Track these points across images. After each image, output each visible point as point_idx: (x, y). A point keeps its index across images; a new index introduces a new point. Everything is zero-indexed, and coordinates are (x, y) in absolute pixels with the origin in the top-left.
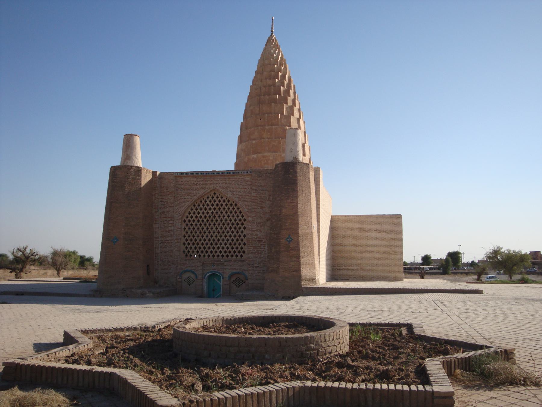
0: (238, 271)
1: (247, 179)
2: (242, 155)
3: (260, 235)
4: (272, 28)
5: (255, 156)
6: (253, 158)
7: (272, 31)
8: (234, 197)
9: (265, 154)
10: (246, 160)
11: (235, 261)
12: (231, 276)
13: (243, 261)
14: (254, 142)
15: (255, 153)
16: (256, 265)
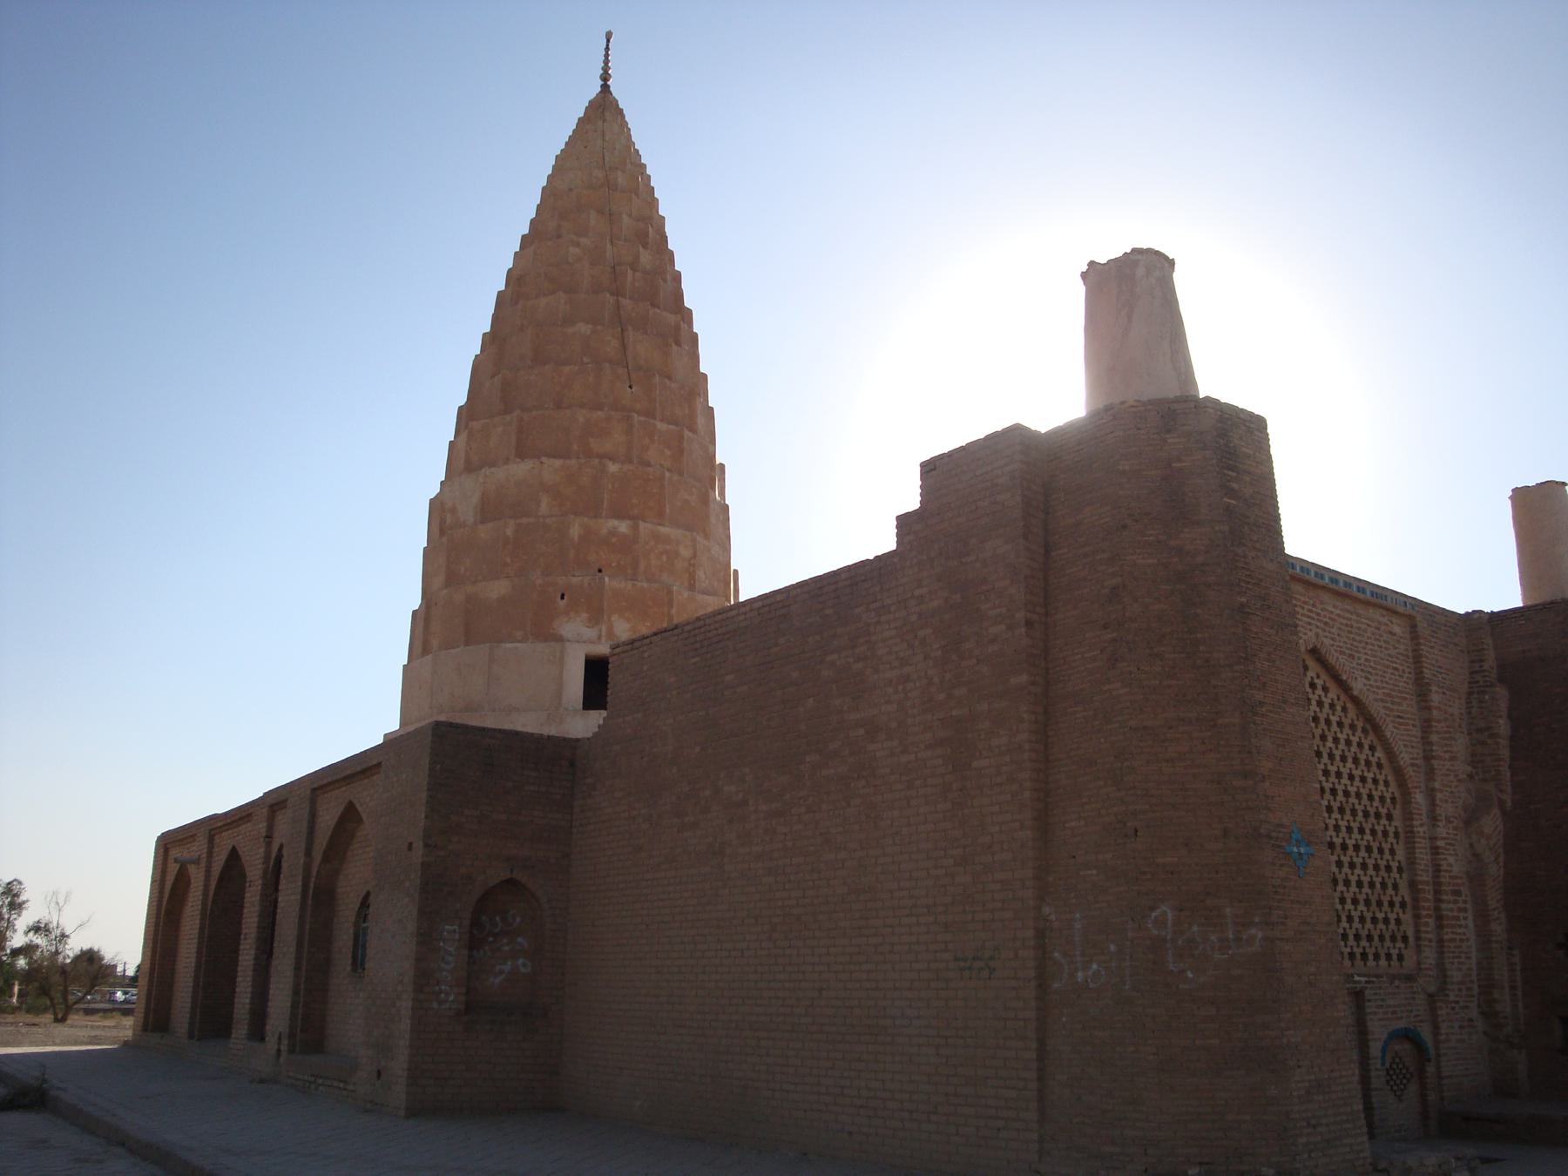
0: (1402, 1024)
1: (1397, 630)
2: (544, 507)
3: (1456, 869)
4: (606, 69)
5: (624, 527)
6: (613, 533)
7: (605, 77)
8: (1372, 696)
9: (661, 529)
10: (575, 531)
11: (1393, 978)
12: (1384, 1050)
13: (1409, 978)
14: (613, 468)
15: (620, 516)
16: (1452, 998)
